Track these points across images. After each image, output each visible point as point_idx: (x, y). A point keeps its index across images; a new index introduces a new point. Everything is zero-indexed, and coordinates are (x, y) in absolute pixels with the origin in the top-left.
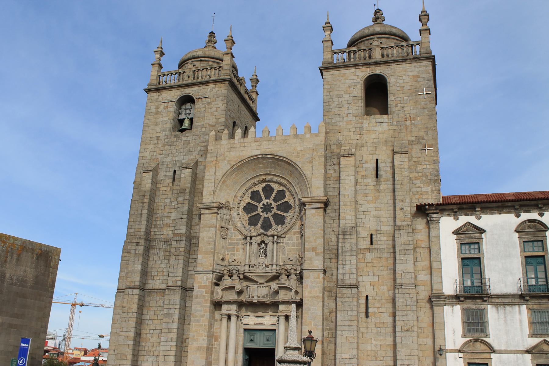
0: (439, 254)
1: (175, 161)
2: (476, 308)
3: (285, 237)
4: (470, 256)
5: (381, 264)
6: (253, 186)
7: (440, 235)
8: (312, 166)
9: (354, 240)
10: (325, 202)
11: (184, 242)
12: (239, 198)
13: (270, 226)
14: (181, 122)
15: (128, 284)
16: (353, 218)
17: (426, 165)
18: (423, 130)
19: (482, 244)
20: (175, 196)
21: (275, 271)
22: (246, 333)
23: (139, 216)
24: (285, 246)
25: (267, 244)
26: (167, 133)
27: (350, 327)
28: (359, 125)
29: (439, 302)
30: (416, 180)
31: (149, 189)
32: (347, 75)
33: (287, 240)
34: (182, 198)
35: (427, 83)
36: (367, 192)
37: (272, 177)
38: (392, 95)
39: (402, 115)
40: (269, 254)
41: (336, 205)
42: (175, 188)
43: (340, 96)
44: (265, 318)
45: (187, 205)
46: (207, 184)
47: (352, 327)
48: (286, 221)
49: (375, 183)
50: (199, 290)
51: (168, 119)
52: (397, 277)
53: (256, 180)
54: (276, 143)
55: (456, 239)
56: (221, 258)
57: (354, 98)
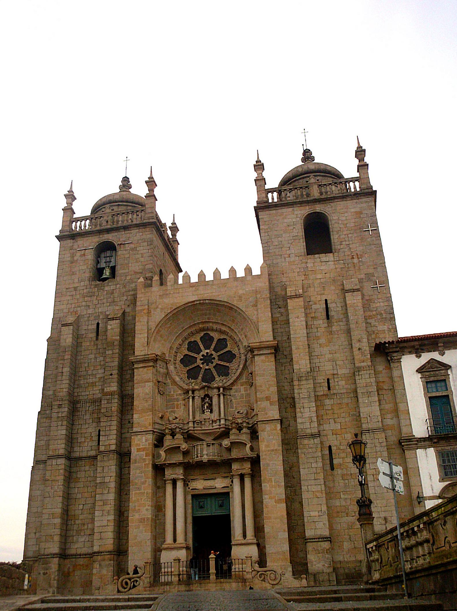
0: (404, 395)
1: (97, 313)
2: (451, 449)
3: (231, 389)
4: (438, 394)
5: (342, 410)
6: (189, 335)
7: (403, 374)
8: (257, 310)
9: (312, 386)
10: (275, 347)
11: (116, 401)
12: (175, 350)
13: (213, 379)
14: (100, 271)
15: (51, 453)
16: (308, 362)
17: (380, 302)
18: (372, 267)
19: (449, 381)
20: (101, 351)
21: (224, 426)
22: (194, 499)
23: (60, 374)
24: (233, 398)
25: (212, 397)
26: (87, 283)
27: (316, 481)
28: (304, 265)
29: (411, 446)
30: (369, 319)
31: (70, 344)
32: (285, 214)
33: (234, 392)
34: (110, 352)
35: (371, 219)
37: (211, 324)
38: (335, 233)
40: (215, 408)
41: (286, 351)
42: (99, 342)
44: (216, 480)
45: (117, 359)
46: (139, 335)
47: (319, 481)
48: (230, 371)
49: (326, 325)
50: (137, 453)
51: (86, 268)
52: (362, 422)
53: (193, 329)
54: (214, 287)
55: (421, 378)
56: (160, 416)
57: (295, 238)
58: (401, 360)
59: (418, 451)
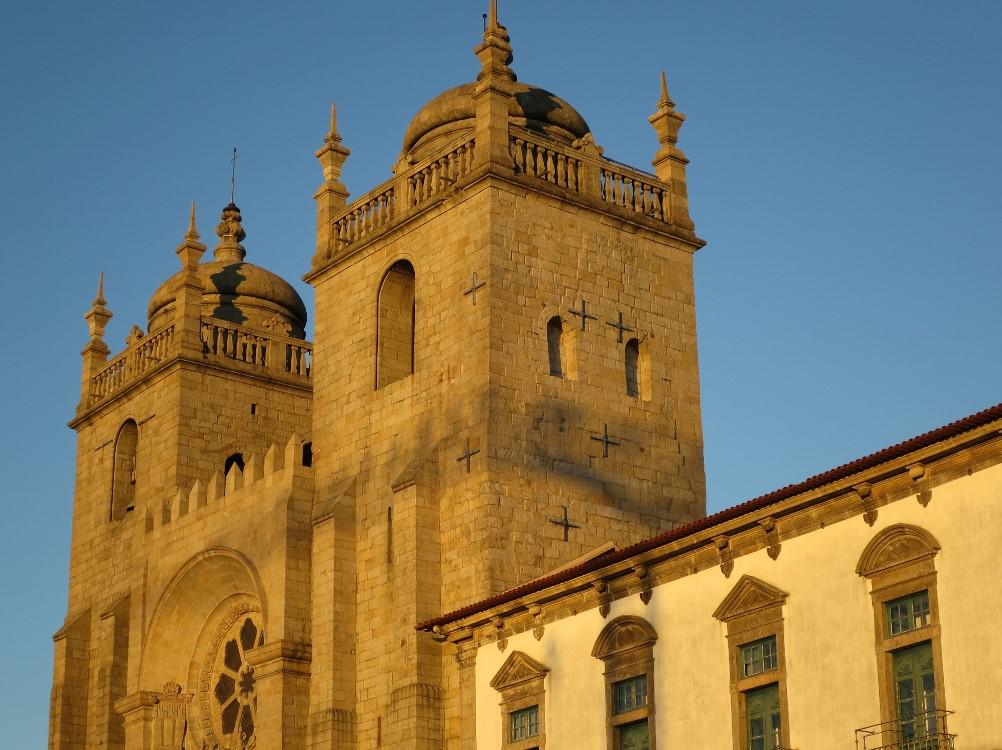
26: (103, 526)
30: (451, 549)
36: (374, 604)
37: (245, 599)
39: (436, 368)
43: (337, 348)
49: (382, 579)
54: (226, 514)
58: (477, 659)
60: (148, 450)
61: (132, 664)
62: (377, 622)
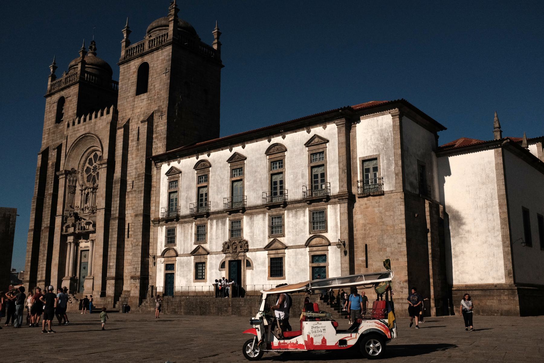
45: (54, 174)
59: (159, 227)
60: (68, 105)
61: (62, 162)
62: (134, 156)
